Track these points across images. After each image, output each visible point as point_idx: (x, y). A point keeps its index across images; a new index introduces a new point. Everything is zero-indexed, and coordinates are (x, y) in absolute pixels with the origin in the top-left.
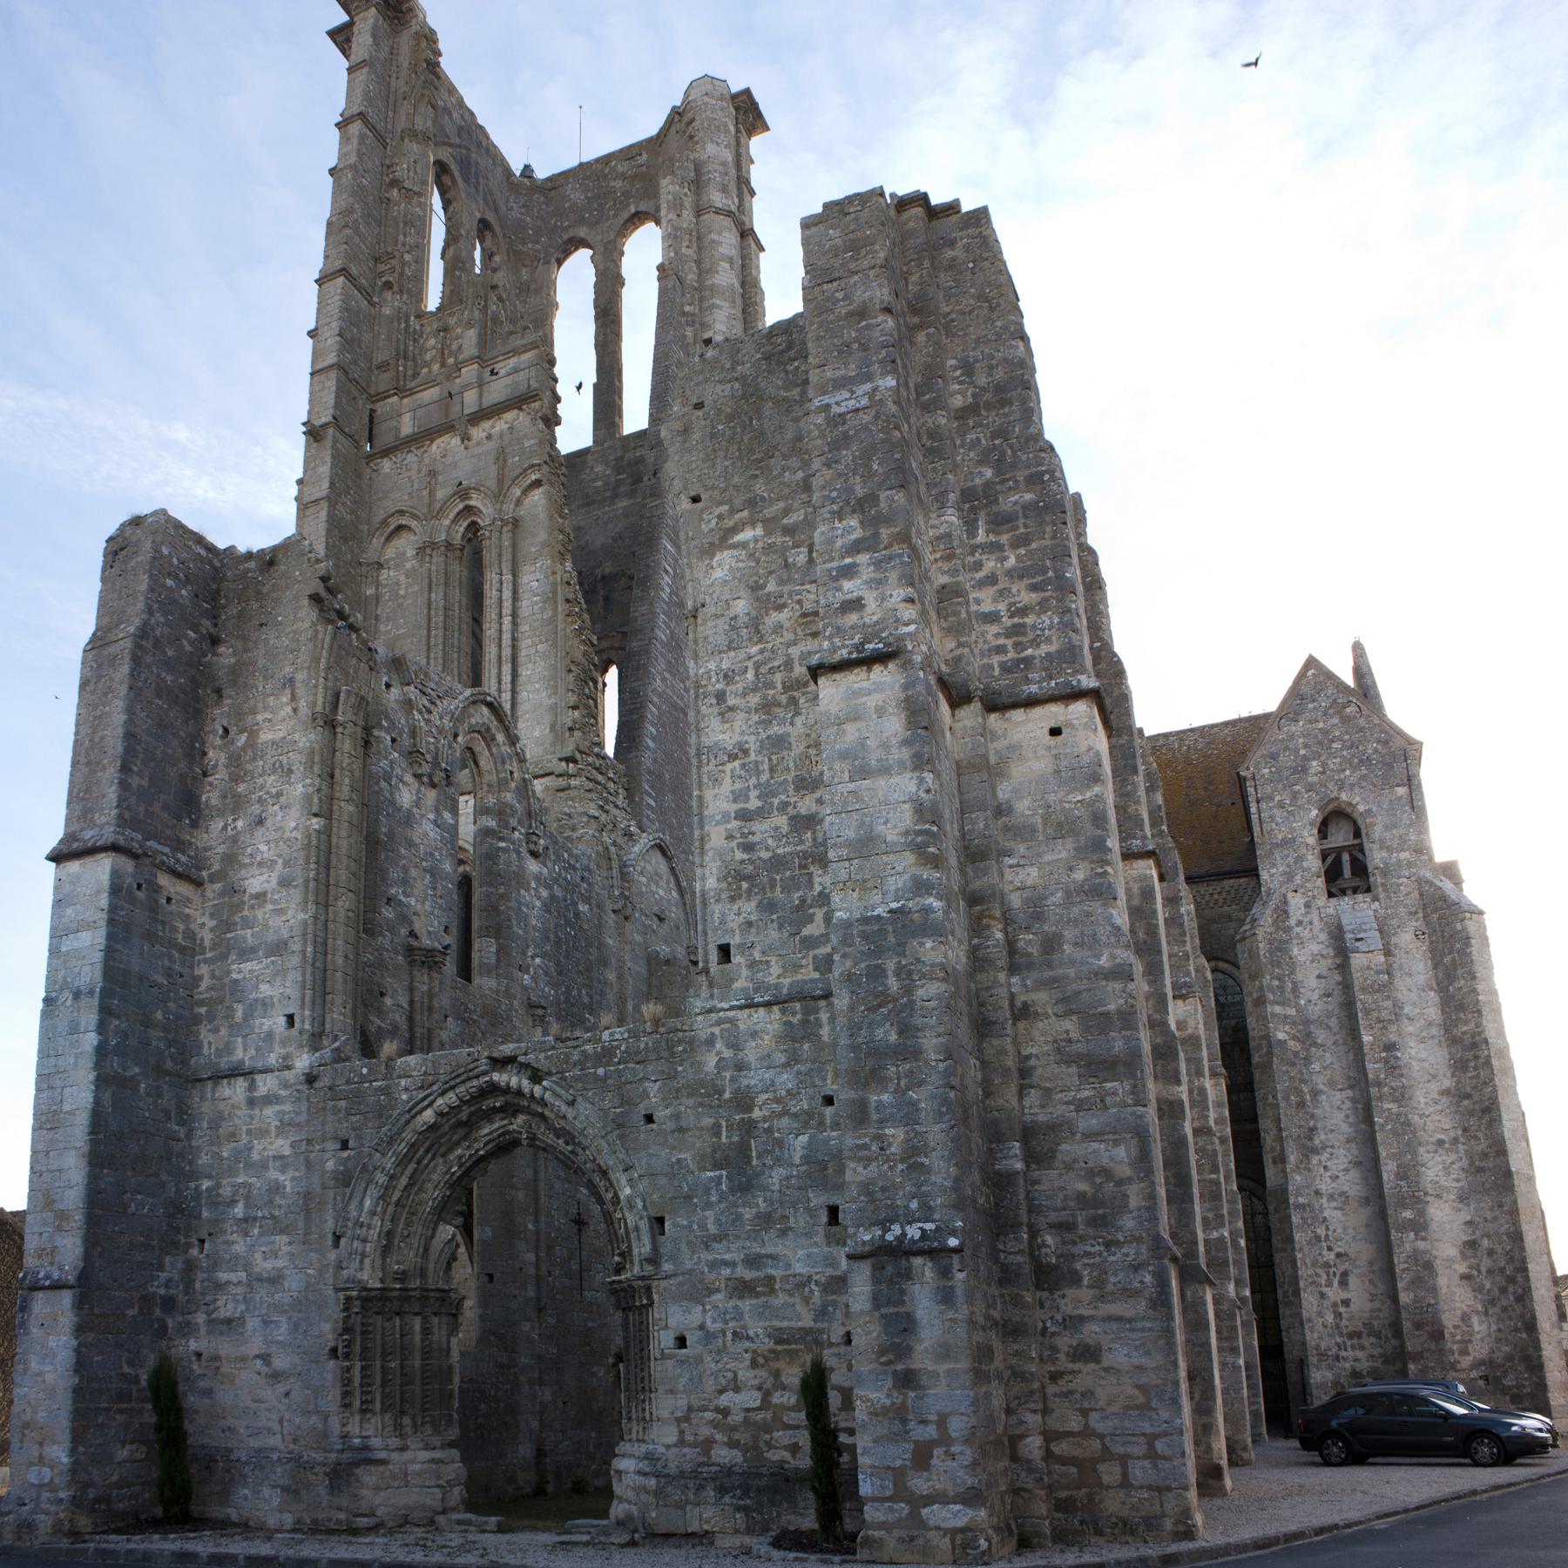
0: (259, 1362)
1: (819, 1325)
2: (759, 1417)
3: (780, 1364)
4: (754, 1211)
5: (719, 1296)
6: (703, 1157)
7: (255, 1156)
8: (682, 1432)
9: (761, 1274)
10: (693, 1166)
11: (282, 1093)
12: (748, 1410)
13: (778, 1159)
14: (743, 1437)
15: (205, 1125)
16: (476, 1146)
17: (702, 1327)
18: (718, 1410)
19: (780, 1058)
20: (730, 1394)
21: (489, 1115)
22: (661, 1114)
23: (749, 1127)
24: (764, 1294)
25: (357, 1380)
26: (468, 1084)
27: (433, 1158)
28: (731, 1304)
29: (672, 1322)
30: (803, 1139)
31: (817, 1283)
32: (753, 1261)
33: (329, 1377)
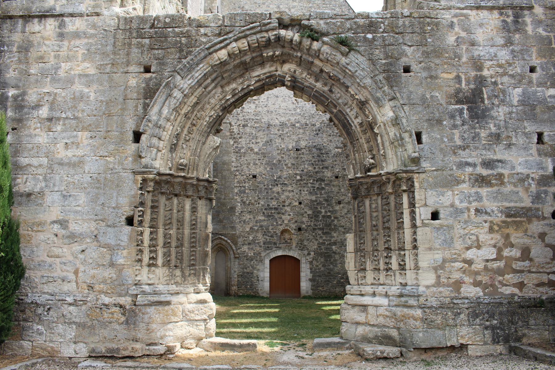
0: (56, 227)
1: (536, 206)
2: (496, 265)
3: (510, 230)
4: (488, 132)
5: (464, 185)
6: (449, 96)
7: (62, 73)
8: (438, 277)
9: (495, 172)
10: (443, 102)
11: (92, 31)
12: (487, 261)
13: (503, 101)
14: (484, 279)
15: (15, 49)
16: (246, 83)
17: (452, 205)
18: (465, 261)
19: (501, 41)
20: (474, 250)
21: (262, 64)
22: (414, 67)
23: (481, 81)
24: (496, 185)
25: (146, 242)
26: (258, 36)
27: (215, 87)
28: (473, 190)
29: (430, 201)
30: (519, 90)
31: (533, 179)
32: (488, 164)
33: (125, 238)
